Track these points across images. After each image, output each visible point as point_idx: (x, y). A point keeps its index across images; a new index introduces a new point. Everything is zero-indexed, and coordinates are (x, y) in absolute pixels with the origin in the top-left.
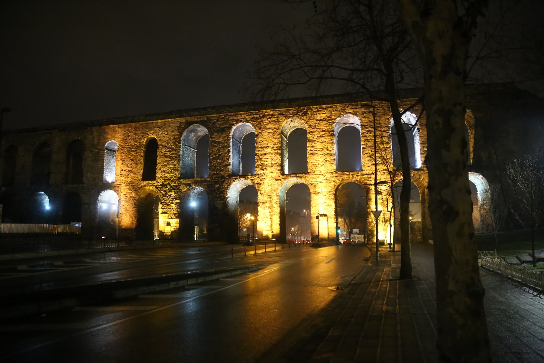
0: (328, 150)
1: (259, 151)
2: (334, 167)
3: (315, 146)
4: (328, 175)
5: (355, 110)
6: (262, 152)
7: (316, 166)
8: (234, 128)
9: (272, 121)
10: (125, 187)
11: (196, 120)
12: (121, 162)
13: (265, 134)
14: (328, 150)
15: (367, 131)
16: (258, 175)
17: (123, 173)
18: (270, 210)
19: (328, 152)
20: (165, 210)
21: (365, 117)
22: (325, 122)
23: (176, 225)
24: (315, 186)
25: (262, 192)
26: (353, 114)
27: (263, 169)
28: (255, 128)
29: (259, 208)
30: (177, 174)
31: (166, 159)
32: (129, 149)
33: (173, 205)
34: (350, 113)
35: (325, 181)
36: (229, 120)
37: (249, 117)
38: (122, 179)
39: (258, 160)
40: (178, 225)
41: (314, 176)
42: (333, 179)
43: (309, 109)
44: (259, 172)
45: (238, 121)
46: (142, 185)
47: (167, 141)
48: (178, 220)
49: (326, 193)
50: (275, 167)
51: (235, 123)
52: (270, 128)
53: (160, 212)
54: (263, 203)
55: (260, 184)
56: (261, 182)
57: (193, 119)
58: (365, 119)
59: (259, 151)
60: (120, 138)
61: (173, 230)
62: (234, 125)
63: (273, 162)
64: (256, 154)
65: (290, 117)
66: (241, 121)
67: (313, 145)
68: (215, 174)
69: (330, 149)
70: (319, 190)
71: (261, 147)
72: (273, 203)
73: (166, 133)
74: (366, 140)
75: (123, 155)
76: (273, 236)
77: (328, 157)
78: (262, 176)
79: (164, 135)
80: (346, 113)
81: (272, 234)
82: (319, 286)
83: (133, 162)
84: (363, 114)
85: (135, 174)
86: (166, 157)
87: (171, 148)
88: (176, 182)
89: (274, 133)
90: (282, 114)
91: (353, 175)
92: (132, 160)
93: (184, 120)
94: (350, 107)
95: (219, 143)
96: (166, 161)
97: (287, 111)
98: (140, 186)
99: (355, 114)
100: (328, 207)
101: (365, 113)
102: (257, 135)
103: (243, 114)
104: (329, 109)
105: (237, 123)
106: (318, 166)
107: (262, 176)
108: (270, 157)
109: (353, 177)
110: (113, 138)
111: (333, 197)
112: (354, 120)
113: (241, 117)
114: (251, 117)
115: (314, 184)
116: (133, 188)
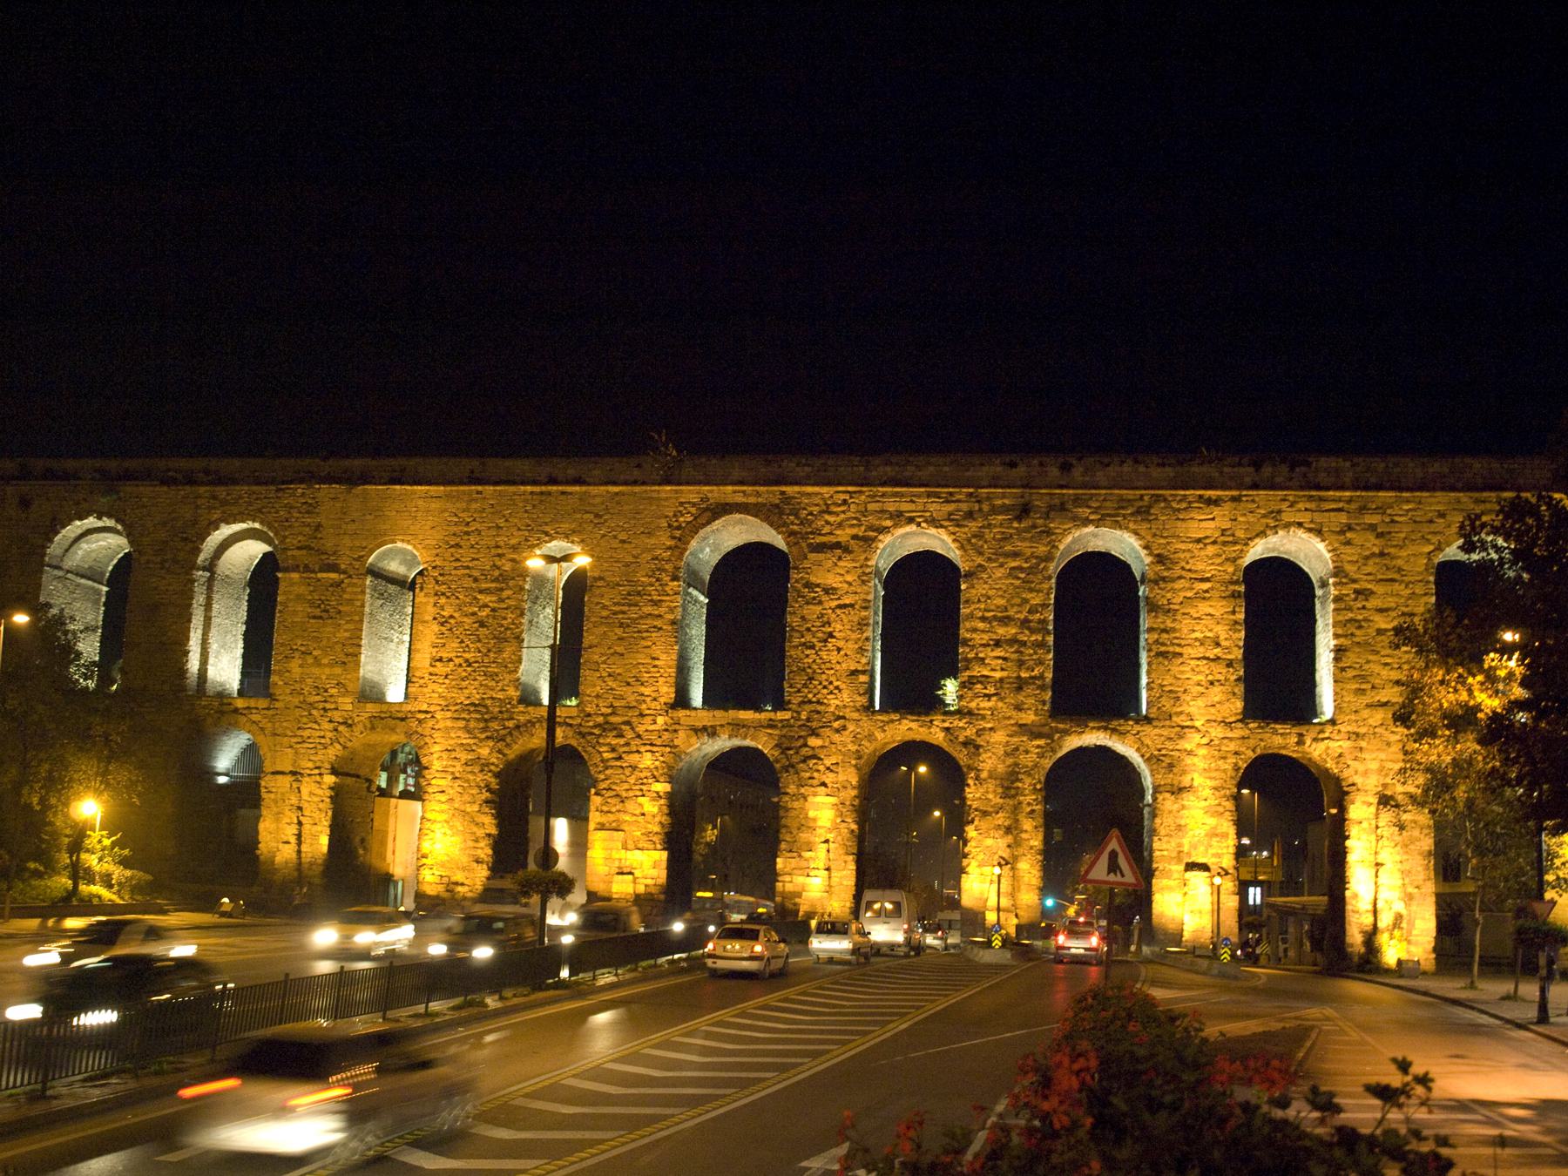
0: (1218, 644)
1: (975, 630)
2: (1239, 705)
3: (1174, 630)
4: (1217, 732)
5: (1318, 517)
6: (986, 637)
7: (1178, 698)
8: (886, 539)
9: (1026, 530)
10: (449, 723)
11: (740, 499)
12: (436, 627)
13: (999, 573)
14: (1218, 644)
15: (1357, 592)
16: (970, 713)
17: (441, 669)
18: (1010, 839)
19: (1217, 651)
20: (611, 817)
21: (1348, 543)
22: (1211, 550)
23: (654, 873)
24: (1171, 766)
25: (984, 775)
26: (1310, 530)
27: (989, 696)
28: (962, 547)
29: (971, 832)
30: (664, 689)
31: (619, 631)
32: (468, 583)
33: (641, 800)
34: (1300, 525)
35: (1203, 752)
36: (865, 513)
37: (937, 508)
38: (434, 694)
39: (967, 660)
40: (664, 874)
41: (1165, 732)
42: (1232, 746)
43: (1157, 499)
44: (973, 705)
45: (899, 518)
46: (522, 718)
47: (627, 565)
48: (665, 854)
49: (1207, 792)
50: (1029, 690)
51: (888, 523)
52: (1015, 555)
53: (592, 826)
54: (985, 814)
55: (977, 747)
56: (979, 741)
57: (729, 493)
58: (1348, 550)
59: (975, 630)
60: (434, 538)
61: (641, 889)
62: (883, 530)
63: (1023, 675)
64: (965, 642)
65: (1086, 522)
66: (911, 520)
67: (1169, 624)
68: (810, 702)
69: (1223, 643)
70: (1186, 781)
71: (983, 619)
72: (1021, 817)
73: (623, 536)
74: (1351, 620)
75: (443, 600)
76: (1018, 927)
77: (1220, 672)
78: (984, 717)
79: (615, 544)
80: (1287, 526)
81: (1015, 921)
82: (1543, 991)
83: (483, 631)
84: (1342, 532)
85: (493, 676)
86: (621, 625)
87: (639, 593)
88: (660, 720)
89: (1031, 571)
90: (1062, 508)
91: (1301, 735)
92: (482, 624)
93: (691, 493)
94: (1301, 506)
95: (828, 591)
96: (621, 639)
97: (1077, 501)
98: (511, 724)
99: (1318, 532)
100: (1214, 841)
101: (1350, 528)
102: (969, 575)
103: (919, 496)
104: (1228, 506)
105: (895, 526)
106: (1183, 697)
107: (984, 717)
108: (1015, 656)
109: (1300, 743)
110: (408, 536)
111: (1230, 805)
112: (1309, 551)
113: (912, 507)
114: (951, 507)
115: (1168, 761)
116: (485, 729)
